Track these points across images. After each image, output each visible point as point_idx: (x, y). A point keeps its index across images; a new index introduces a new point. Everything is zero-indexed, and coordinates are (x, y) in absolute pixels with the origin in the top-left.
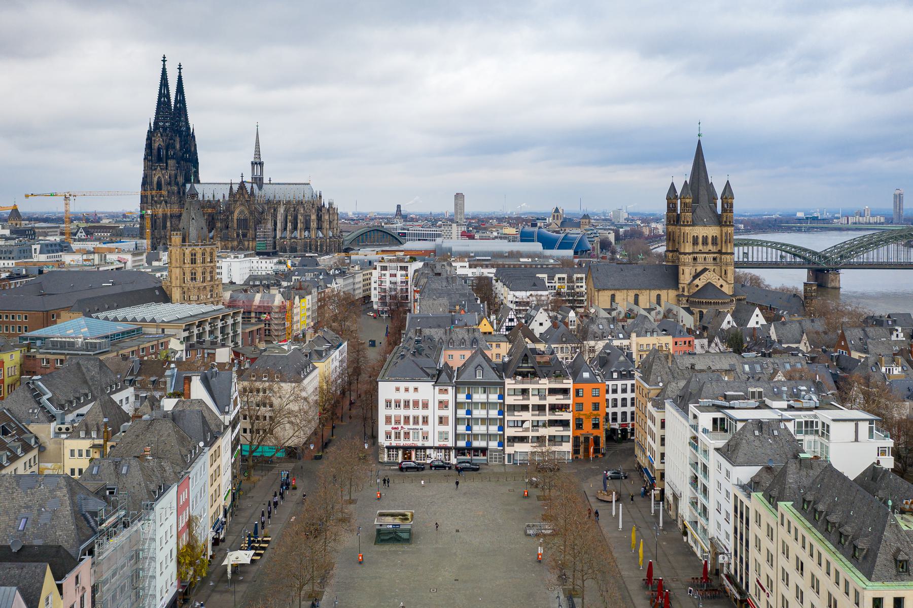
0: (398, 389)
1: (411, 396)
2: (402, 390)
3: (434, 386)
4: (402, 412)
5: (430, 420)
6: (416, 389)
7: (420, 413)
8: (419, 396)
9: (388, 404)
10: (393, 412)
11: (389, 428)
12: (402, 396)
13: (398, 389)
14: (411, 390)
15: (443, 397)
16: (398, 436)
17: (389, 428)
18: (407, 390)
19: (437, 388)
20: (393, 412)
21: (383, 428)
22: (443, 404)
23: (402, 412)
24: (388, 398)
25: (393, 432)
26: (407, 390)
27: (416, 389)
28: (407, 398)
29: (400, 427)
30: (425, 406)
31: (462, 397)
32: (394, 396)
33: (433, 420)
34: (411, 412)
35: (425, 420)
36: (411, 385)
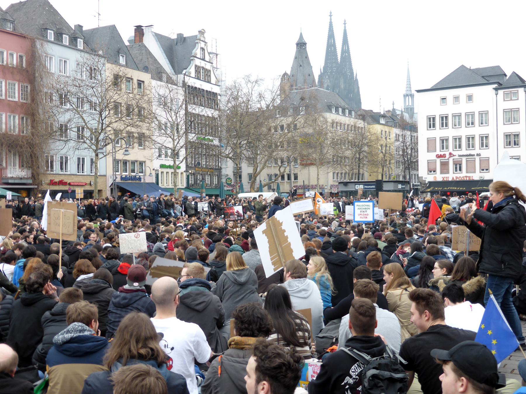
1: (463, 108)
2: (450, 100)
3: (496, 89)
4: (450, 133)
5: (492, 142)
6: (470, 98)
7: (477, 131)
8: (475, 107)
9: (431, 123)
10: (438, 133)
11: (432, 156)
12: (450, 109)
16: (444, 166)
17: (432, 156)
18: (457, 99)
19: (501, 92)
20: (438, 133)
21: (424, 157)
23: (450, 133)
24: (431, 113)
25: (438, 161)
26: (457, 99)
27: (470, 98)
28: (457, 111)
32: (438, 111)
33: (497, 141)
34: (464, 132)
35: (484, 140)
36: (463, 92)
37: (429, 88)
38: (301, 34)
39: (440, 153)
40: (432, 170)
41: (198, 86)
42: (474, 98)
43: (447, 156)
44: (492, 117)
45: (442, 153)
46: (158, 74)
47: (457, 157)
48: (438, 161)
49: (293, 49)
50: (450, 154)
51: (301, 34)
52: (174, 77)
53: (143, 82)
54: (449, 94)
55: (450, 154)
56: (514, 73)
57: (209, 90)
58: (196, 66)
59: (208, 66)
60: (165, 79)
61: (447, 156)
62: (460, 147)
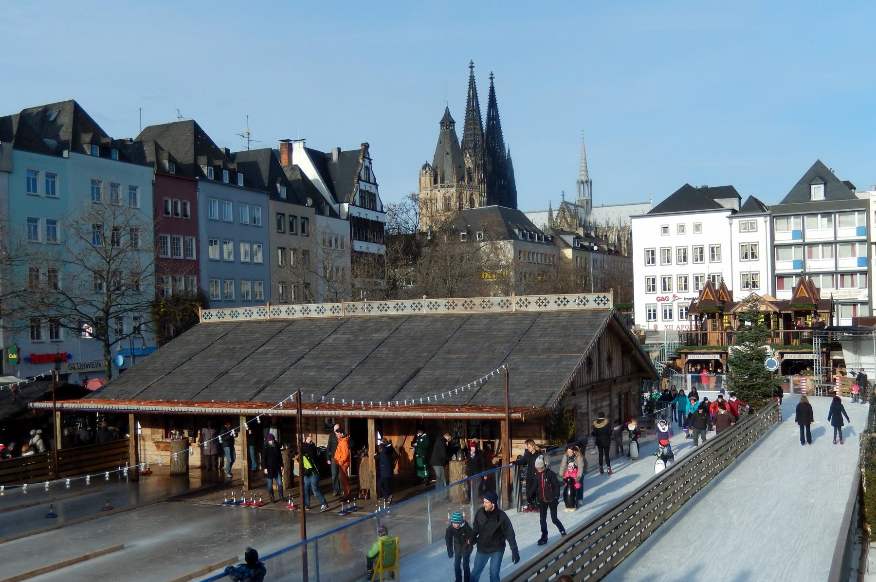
0: (665, 229)
1: (690, 240)
2: (673, 229)
4: (674, 270)
6: (697, 227)
8: (705, 240)
10: (658, 271)
12: (674, 241)
13: (665, 229)
14: (689, 228)
15: (749, 238)
17: (652, 298)
18: (682, 229)
19: (736, 221)
22: (749, 253)
23: (674, 270)
24: (650, 246)
26: (682, 229)
27: (697, 227)
29: (670, 296)
30: (714, 252)
31: (784, 236)
32: (658, 242)
36: (689, 219)
37: (645, 213)
38: (447, 109)
39: (661, 295)
40: (652, 315)
41: (363, 216)
42: (704, 227)
43: (671, 299)
44: (725, 252)
45: (664, 295)
46: (320, 205)
47: (682, 301)
48: (659, 304)
49: (437, 130)
50: (674, 296)
51: (447, 109)
52: (335, 207)
53: (307, 219)
54: (673, 220)
55: (674, 296)
56: (751, 197)
57: (375, 219)
58: (361, 191)
59: (373, 190)
60: (327, 212)
61: (671, 299)
62: (686, 287)
